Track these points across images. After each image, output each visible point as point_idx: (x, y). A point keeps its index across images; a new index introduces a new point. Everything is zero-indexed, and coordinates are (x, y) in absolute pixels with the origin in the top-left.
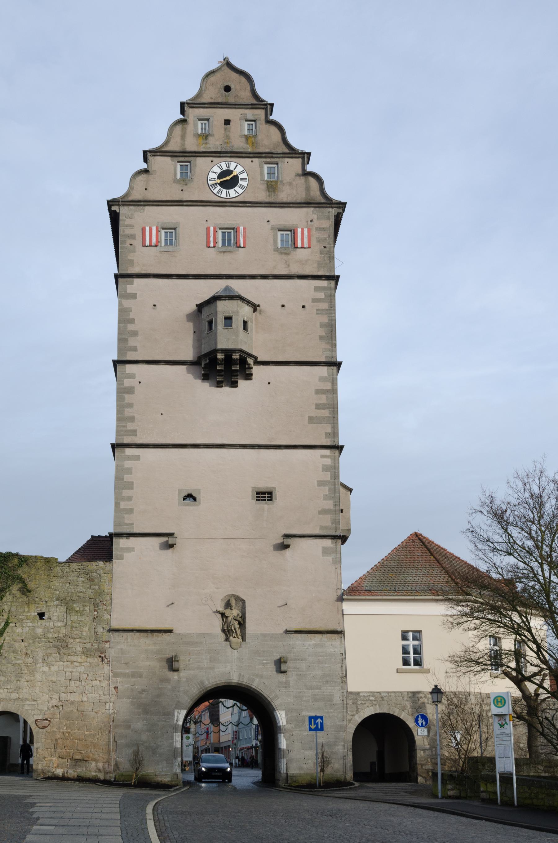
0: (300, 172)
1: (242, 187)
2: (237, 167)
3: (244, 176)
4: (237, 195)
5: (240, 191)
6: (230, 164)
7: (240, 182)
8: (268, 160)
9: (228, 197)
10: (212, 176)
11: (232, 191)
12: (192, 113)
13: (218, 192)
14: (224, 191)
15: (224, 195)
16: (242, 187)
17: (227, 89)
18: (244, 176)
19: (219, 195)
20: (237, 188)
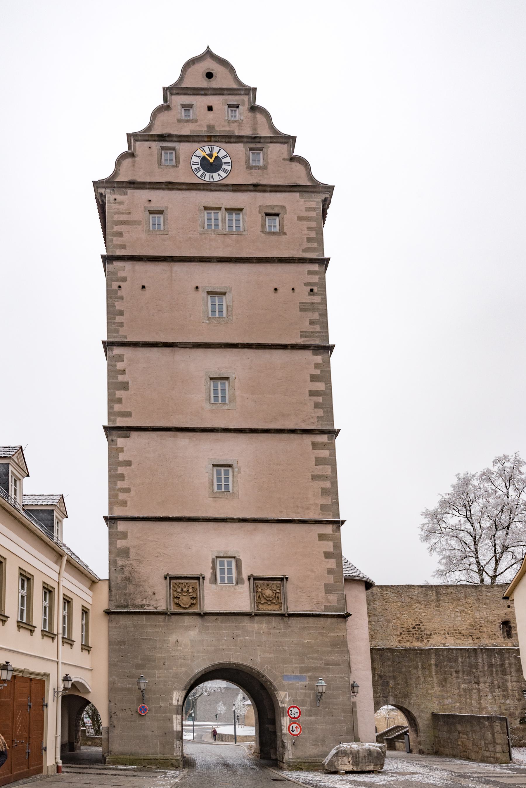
0: (286, 156)
1: (225, 171)
2: (219, 151)
3: (228, 160)
4: (221, 178)
5: (224, 175)
6: (213, 148)
7: (224, 166)
8: (252, 145)
9: (212, 180)
10: (195, 159)
11: (215, 175)
12: (177, 100)
13: (202, 176)
14: (208, 174)
15: (207, 178)
16: (225, 171)
17: (209, 75)
18: (228, 160)
19: (203, 178)
20: (220, 172)
